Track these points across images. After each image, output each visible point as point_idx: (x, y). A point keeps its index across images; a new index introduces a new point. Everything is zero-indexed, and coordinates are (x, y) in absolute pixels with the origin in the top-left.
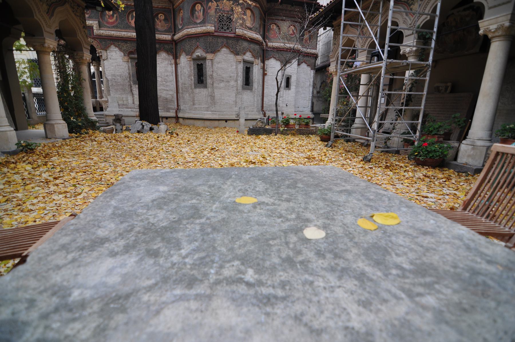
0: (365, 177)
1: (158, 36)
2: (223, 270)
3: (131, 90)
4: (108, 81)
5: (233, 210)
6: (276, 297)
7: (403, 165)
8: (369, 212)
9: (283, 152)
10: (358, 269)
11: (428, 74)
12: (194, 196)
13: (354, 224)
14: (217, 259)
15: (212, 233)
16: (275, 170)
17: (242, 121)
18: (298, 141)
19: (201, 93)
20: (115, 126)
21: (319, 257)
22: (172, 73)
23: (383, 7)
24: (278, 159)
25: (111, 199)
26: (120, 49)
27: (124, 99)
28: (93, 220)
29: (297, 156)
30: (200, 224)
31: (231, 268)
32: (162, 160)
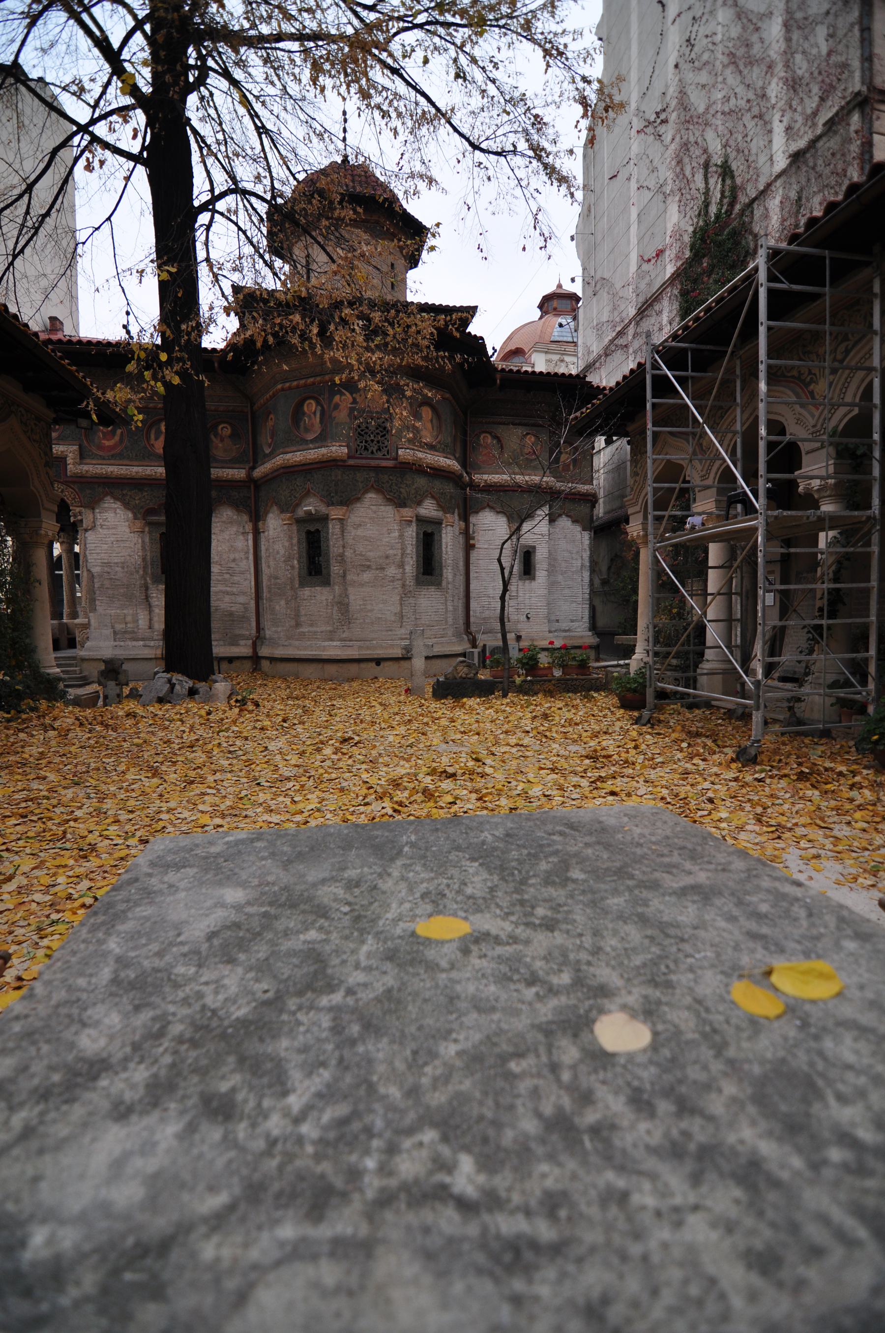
0: (748, 806)
1: (217, 473)
2: (398, 1159)
3: (147, 597)
4: (92, 576)
5: (412, 962)
6: (534, 1245)
7: (843, 768)
8: (758, 956)
9: (526, 741)
10: (740, 1148)
11: (875, 538)
12: (311, 918)
13: (722, 999)
14: (379, 1124)
15: (362, 1039)
16: (510, 825)
17: (418, 663)
18: (563, 710)
19: (317, 599)
20: (105, 686)
21: (639, 1110)
22: (247, 552)
23: (742, 390)
24: (514, 763)
25: (108, 933)
26: (127, 506)
27: (129, 619)
28: (66, 1003)
29: (562, 752)
30: (331, 1009)
31: (415, 1153)
32: (218, 776)
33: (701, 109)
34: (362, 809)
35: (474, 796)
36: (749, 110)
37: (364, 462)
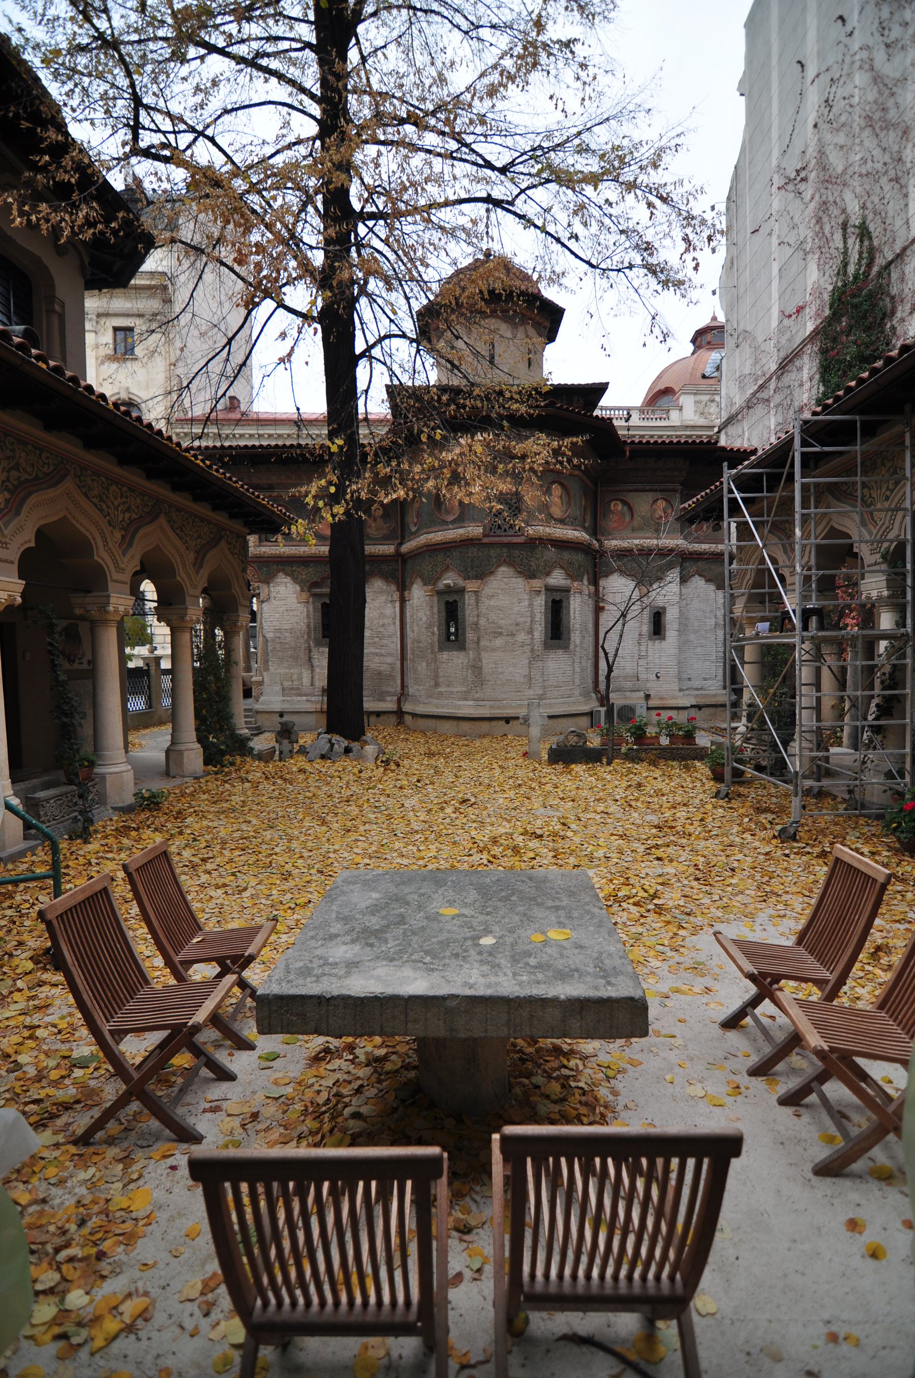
1: (370, 549)
3: (310, 658)
4: (266, 641)
9: (613, 808)
17: (535, 731)
19: (454, 662)
22: (394, 618)
26: (295, 580)
27: (295, 677)
32: (367, 827)
33: (839, 170)
34: (466, 858)
35: (552, 854)
36: (886, 172)
37: (497, 539)
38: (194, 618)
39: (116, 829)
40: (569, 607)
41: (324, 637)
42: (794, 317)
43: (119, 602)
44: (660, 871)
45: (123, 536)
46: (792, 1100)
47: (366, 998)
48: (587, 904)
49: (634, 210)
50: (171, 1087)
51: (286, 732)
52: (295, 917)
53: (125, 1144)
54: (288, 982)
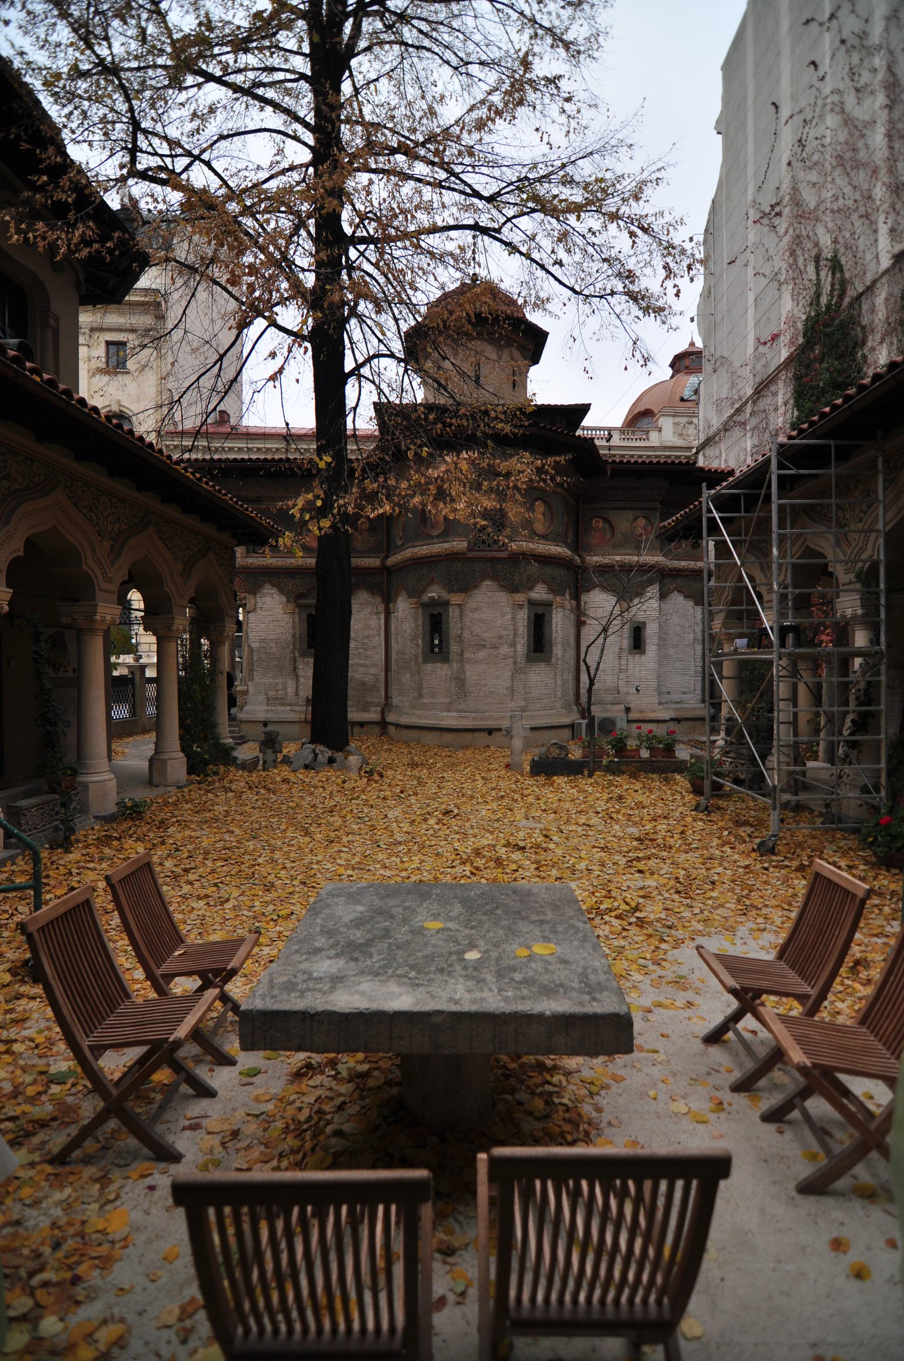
1: (356, 562)
3: (295, 668)
4: (251, 651)
9: (595, 821)
17: (517, 743)
19: (438, 674)
20: (264, 754)
22: (379, 630)
26: (281, 591)
27: (280, 687)
32: (350, 838)
33: (812, 206)
34: (449, 870)
35: (534, 866)
36: (857, 208)
37: (482, 554)
38: (181, 628)
39: (98, 839)
40: (551, 621)
41: (309, 647)
42: (769, 344)
43: (107, 611)
44: (641, 884)
45: (112, 546)
46: (774, 1116)
47: (350, 1014)
48: (571, 918)
49: (617, 239)
50: (150, 1103)
51: (270, 742)
52: (278, 928)
53: (103, 1163)
54: (272, 997)
